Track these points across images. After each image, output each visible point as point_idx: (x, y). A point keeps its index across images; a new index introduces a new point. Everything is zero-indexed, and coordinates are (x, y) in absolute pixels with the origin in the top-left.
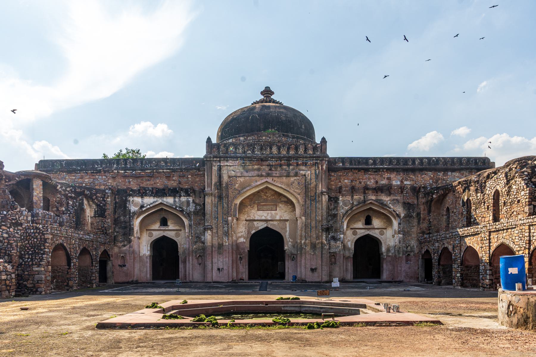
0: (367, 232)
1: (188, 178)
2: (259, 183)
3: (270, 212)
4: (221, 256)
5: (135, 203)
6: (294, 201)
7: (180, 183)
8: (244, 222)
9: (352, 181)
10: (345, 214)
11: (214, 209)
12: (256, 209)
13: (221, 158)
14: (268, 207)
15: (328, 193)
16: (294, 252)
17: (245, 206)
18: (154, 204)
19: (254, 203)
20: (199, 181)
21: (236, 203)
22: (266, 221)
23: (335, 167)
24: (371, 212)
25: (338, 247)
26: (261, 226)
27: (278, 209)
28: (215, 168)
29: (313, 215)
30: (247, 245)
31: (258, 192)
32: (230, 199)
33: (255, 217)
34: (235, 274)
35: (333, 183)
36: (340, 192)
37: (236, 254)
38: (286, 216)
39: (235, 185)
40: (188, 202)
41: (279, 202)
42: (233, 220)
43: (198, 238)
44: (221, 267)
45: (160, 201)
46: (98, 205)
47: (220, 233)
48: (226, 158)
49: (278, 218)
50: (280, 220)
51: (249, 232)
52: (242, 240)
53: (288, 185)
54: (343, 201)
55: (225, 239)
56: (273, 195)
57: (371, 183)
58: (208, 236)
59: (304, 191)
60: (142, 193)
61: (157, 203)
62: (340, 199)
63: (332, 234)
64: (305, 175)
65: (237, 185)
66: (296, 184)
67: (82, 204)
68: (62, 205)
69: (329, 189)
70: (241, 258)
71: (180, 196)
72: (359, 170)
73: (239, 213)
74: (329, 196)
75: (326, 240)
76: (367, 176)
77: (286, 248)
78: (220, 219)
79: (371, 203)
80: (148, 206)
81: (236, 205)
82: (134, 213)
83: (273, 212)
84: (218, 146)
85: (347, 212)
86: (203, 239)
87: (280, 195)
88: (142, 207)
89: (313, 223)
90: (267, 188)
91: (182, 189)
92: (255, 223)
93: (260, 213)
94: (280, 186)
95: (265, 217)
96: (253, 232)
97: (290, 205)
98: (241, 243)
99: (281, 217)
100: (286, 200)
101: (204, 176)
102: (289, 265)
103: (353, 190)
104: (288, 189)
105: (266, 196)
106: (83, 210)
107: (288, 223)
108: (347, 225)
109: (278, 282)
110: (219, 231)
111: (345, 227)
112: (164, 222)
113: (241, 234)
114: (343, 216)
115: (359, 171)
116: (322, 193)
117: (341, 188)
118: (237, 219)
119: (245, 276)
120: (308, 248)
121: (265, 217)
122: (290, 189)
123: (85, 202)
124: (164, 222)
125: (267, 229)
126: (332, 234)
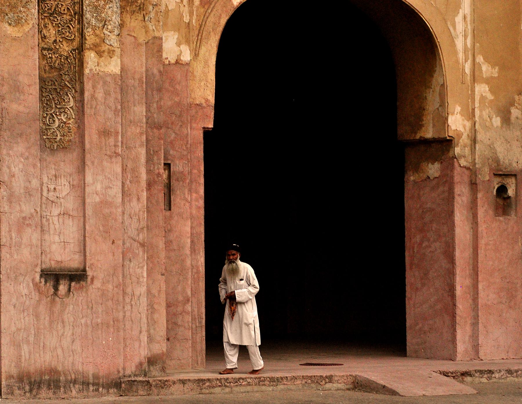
4: (66, 163)
44: (66, 257)
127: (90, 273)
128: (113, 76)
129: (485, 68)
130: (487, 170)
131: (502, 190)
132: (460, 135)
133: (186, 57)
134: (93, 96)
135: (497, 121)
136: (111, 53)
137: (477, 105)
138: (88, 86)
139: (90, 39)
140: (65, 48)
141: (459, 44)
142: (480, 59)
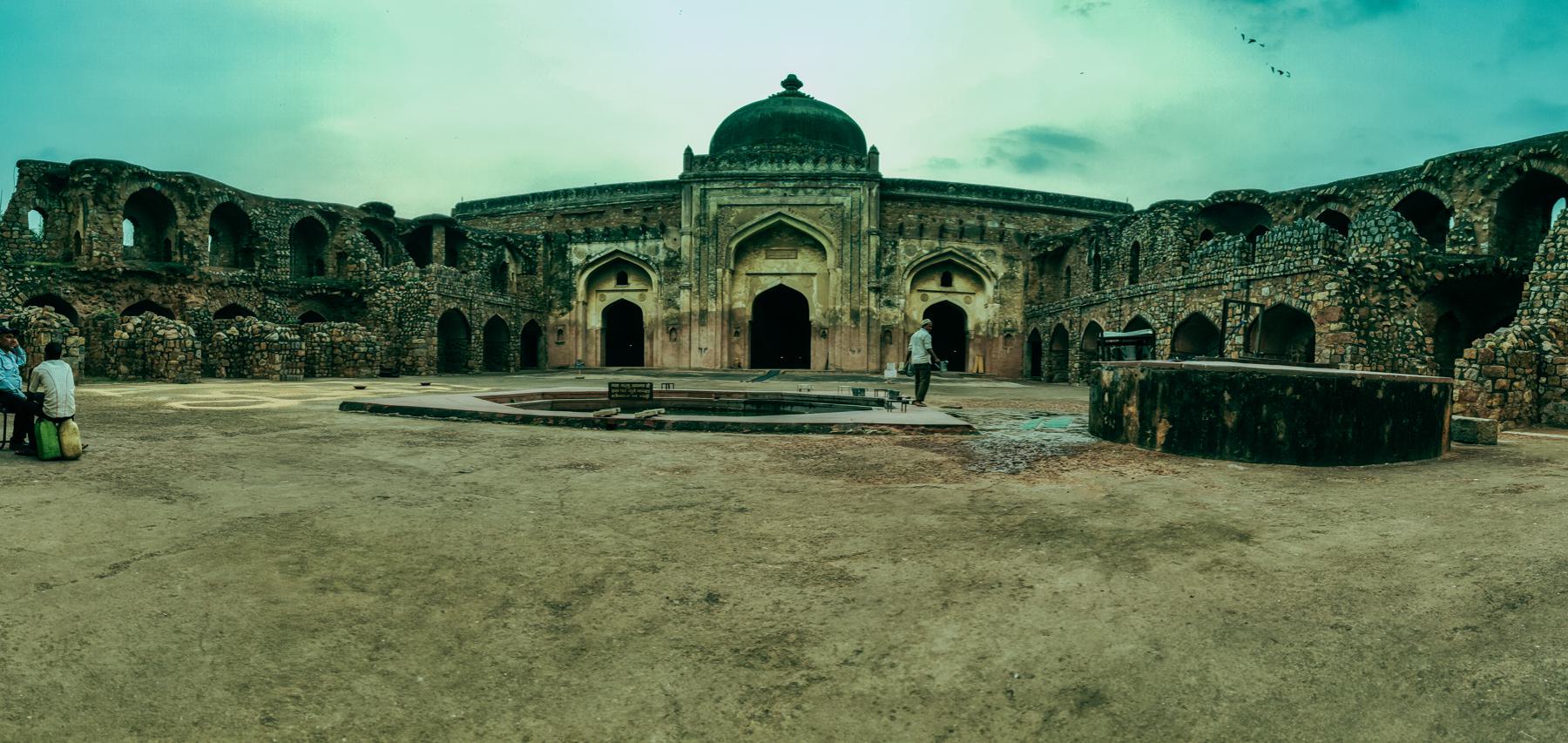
0: (944, 298)
2: (767, 215)
5: (579, 253)
6: (824, 243)
7: (645, 219)
9: (920, 217)
11: (695, 256)
16: (825, 323)
23: (893, 193)
26: (772, 282)
28: (696, 193)
29: (855, 266)
30: (749, 312)
34: (726, 358)
38: (813, 268)
40: (657, 249)
43: (670, 302)
46: (526, 258)
47: (703, 292)
48: (715, 178)
49: (799, 270)
51: (751, 292)
52: (739, 305)
53: (814, 219)
55: (711, 302)
57: (951, 222)
58: (685, 295)
60: (589, 237)
63: (885, 298)
66: (827, 217)
67: (502, 256)
68: (472, 258)
69: (882, 225)
72: (933, 200)
76: (943, 211)
77: (812, 317)
78: (704, 270)
79: (951, 253)
81: (728, 249)
84: (703, 159)
87: (802, 236)
88: (589, 257)
89: (855, 281)
90: (781, 225)
92: (762, 278)
96: (758, 292)
102: (816, 345)
103: (921, 232)
106: (505, 266)
107: (815, 279)
109: (798, 372)
112: (622, 280)
113: (742, 298)
116: (870, 233)
117: (901, 226)
118: (733, 273)
119: (745, 361)
123: (507, 253)
124: (622, 280)
125: (781, 286)
126: (885, 298)
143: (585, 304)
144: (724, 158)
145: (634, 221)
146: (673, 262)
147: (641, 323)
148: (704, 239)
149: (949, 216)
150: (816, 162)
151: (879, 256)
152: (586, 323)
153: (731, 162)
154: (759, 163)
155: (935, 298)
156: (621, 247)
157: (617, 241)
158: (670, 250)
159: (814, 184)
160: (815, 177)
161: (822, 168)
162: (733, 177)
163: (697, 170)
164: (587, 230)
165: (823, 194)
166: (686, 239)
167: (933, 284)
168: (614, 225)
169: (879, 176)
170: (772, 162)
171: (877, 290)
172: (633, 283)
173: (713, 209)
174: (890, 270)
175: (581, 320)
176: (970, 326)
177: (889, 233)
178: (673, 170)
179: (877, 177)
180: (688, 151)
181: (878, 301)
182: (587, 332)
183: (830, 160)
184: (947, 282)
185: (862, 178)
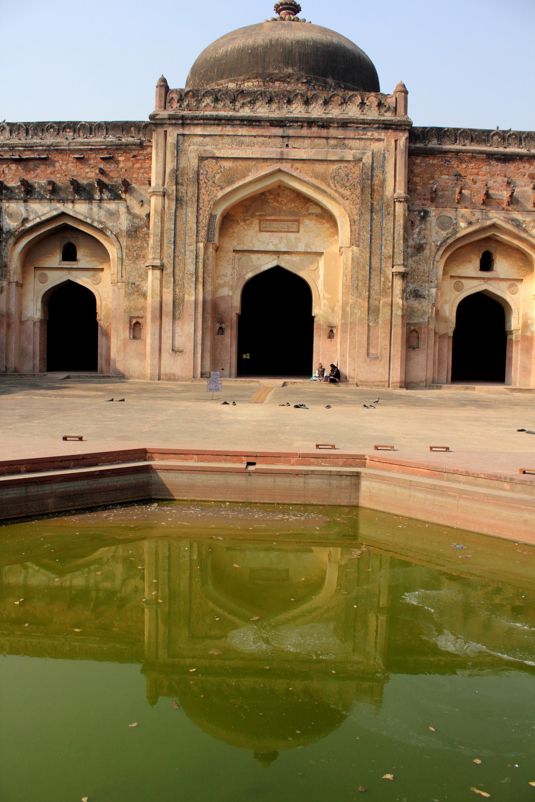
1: (117, 162)
3: (284, 235)
7: (102, 172)
8: (232, 255)
10: (441, 244)
12: (257, 228)
13: (183, 121)
14: (282, 225)
15: (407, 200)
17: (234, 220)
18: (48, 216)
19: (253, 216)
20: (141, 168)
21: (214, 214)
22: (277, 253)
24: (493, 245)
25: (424, 313)
26: (267, 263)
27: (302, 229)
29: (376, 243)
30: (237, 302)
31: (263, 194)
32: (201, 205)
33: (254, 247)
35: (417, 180)
36: (433, 200)
37: (213, 321)
39: (214, 177)
41: (304, 216)
42: (206, 248)
45: (61, 207)
48: (195, 121)
49: (301, 248)
50: (306, 253)
52: (225, 292)
53: (323, 178)
54: (439, 217)
56: (292, 201)
59: (358, 191)
61: (55, 213)
62: (433, 214)
64: (360, 160)
65: (218, 176)
70: (221, 331)
71: (101, 200)
73: (220, 235)
74: (408, 207)
75: (402, 298)
77: (315, 311)
79: (494, 226)
80: (38, 220)
82: (10, 233)
83: (292, 236)
85: (445, 241)
86: (145, 288)
87: (307, 200)
88: (25, 220)
91: (102, 186)
92: (254, 257)
93: (265, 236)
94: (307, 179)
95: (275, 245)
96: (249, 275)
97: (328, 222)
98: (223, 297)
99: (307, 245)
100: (318, 211)
101: (151, 160)
104: (324, 187)
105: (277, 201)
108: (444, 270)
110: (177, 271)
111: (441, 272)
114: (438, 250)
115: (473, 157)
120: (361, 313)
121: (275, 245)
122: (329, 186)
124: (70, 254)
125: (277, 269)
126: (411, 287)
127: (185, 351)
128: (192, 301)
129: (326, 295)
130: (325, 325)
131: (332, 331)
132: (318, 315)
133: (231, 294)
134: (187, 306)
135: (330, 311)
136: (192, 295)
137: (322, 306)
138: (185, 304)
139: (187, 291)
140: (181, 294)
141: (319, 288)
142: (325, 292)
143: (20, 285)
144: (204, 96)
145: (88, 175)
146: (137, 232)
147: (95, 314)
148: (179, 201)
149: (493, 176)
150: (326, 103)
151: (405, 228)
152: (21, 314)
153: (216, 100)
154: (252, 102)
155: (472, 288)
156: (68, 208)
157: (63, 201)
158: (135, 216)
159: (324, 132)
160: (325, 124)
161: (335, 112)
162: (218, 121)
163: (173, 109)
164: (24, 183)
165: (335, 147)
166: (155, 202)
167: (471, 268)
168: (60, 180)
169: (410, 124)
170: (270, 101)
171: (404, 276)
172: (84, 258)
173: (191, 161)
174: (420, 248)
175: (13, 308)
176: (515, 323)
177: (420, 198)
178: (141, 107)
179: (404, 126)
180: (164, 85)
181: (404, 291)
182: (22, 323)
183: (345, 102)
184: (486, 264)
185: (387, 126)
